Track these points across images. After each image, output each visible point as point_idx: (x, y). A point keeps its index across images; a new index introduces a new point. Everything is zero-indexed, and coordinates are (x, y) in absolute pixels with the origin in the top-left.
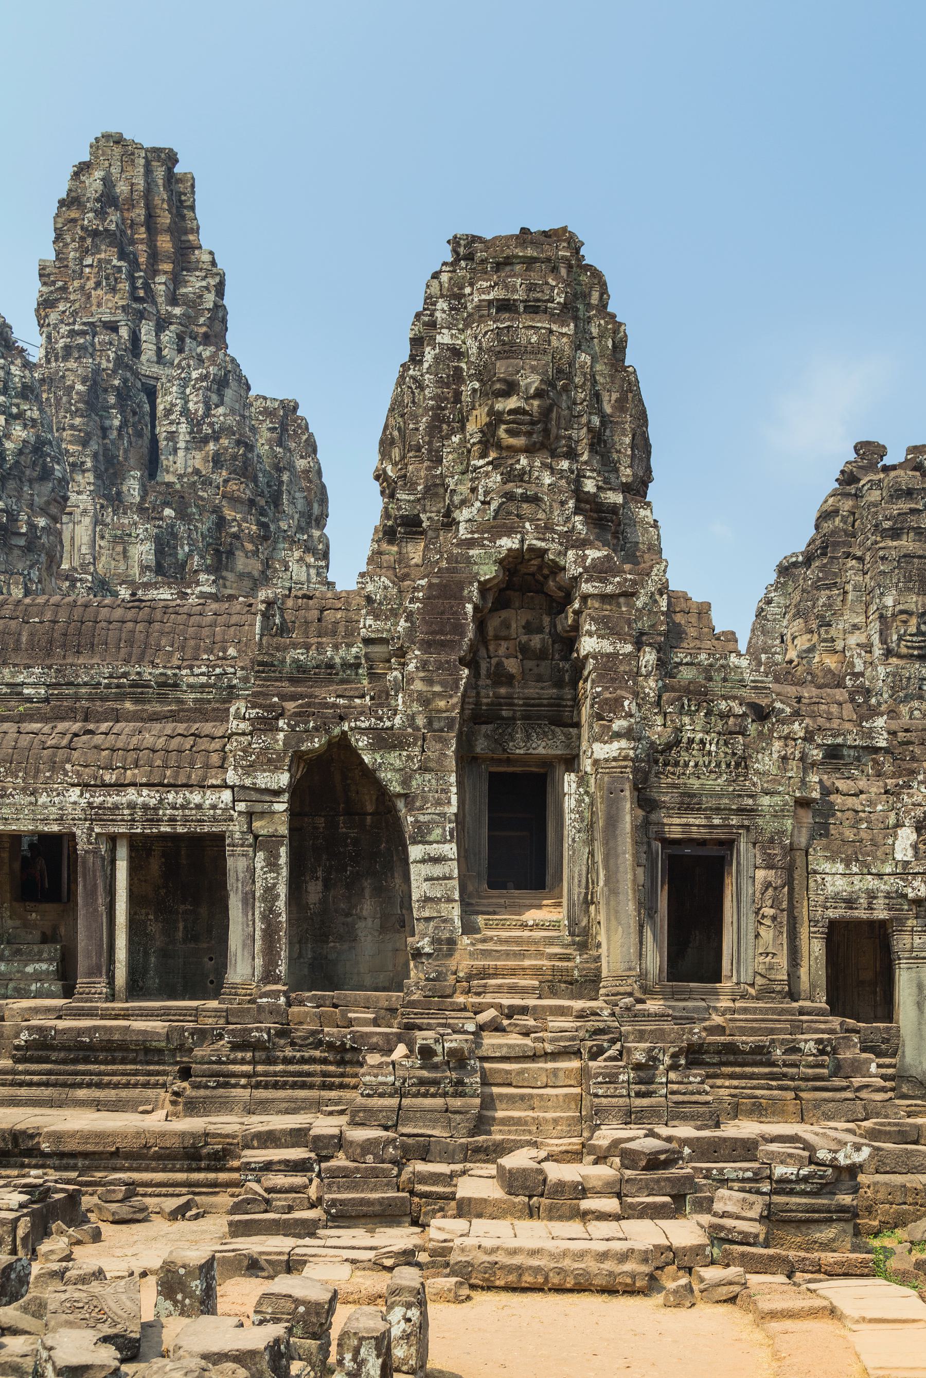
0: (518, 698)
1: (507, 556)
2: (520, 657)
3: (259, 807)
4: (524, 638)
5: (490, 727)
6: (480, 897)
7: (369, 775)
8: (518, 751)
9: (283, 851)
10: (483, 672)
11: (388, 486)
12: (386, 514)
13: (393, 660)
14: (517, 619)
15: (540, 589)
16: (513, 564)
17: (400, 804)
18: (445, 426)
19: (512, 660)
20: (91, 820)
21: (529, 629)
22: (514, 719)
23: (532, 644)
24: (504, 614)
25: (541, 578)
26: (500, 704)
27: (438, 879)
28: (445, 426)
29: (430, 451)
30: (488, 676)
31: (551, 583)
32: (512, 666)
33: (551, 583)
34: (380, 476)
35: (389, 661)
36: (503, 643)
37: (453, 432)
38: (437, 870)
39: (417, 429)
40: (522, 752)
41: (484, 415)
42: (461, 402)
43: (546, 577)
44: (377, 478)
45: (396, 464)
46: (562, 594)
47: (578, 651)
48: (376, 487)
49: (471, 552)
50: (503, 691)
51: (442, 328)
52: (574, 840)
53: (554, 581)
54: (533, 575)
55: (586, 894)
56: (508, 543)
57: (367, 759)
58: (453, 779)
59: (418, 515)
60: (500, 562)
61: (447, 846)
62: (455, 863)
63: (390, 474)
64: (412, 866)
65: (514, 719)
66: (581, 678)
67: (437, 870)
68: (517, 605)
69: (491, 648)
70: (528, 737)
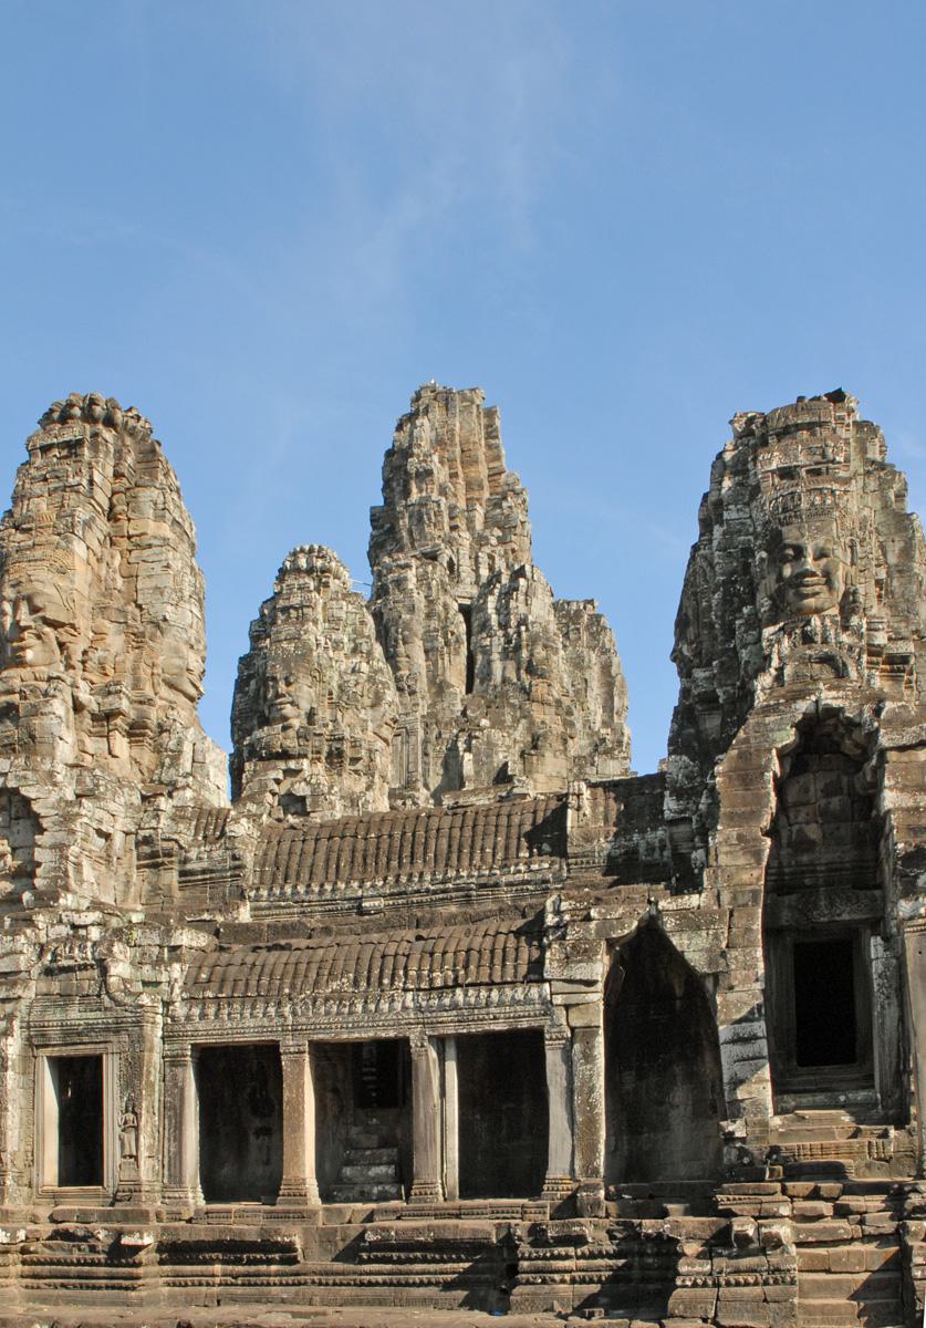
0: (821, 864)
1: (803, 719)
2: (820, 821)
3: (574, 999)
4: (823, 802)
5: (794, 897)
6: (794, 1076)
7: (677, 958)
8: (822, 919)
9: (600, 1040)
10: (784, 841)
11: (685, 665)
12: (685, 693)
13: (696, 839)
14: (815, 783)
15: (836, 749)
16: (808, 726)
17: (709, 984)
18: (736, 599)
19: (814, 826)
20: (424, 1023)
21: (828, 792)
22: (815, 887)
23: (832, 806)
24: (802, 779)
25: (836, 738)
26: (803, 872)
27: (749, 1059)
28: (736, 599)
29: (723, 625)
30: (789, 845)
31: (848, 742)
32: (813, 832)
33: (848, 742)
34: (676, 656)
35: (692, 841)
36: (801, 808)
37: (745, 605)
38: (748, 1050)
39: (710, 606)
40: (826, 919)
41: (773, 582)
42: (750, 573)
43: (842, 736)
44: (674, 660)
45: (692, 643)
46: (859, 751)
47: (878, 811)
48: (674, 667)
49: (767, 720)
50: (805, 858)
51: (729, 504)
52: (883, 1007)
53: (850, 738)
54: (829, 735)
55: (898, 1064)
56: (803, 706)
57: (675, 941)
58: (759, 953)
59: (714, 691)
60: (797, 726)
61: (756, 1024)
62: (765, 1041)
63: (686, 653)
64: (722, 1047)
65: (815, 887)
66: (882, 836)
67: (748, 1050)
68: (815, 768)
69: (792, 815)
70: (832, 904)
